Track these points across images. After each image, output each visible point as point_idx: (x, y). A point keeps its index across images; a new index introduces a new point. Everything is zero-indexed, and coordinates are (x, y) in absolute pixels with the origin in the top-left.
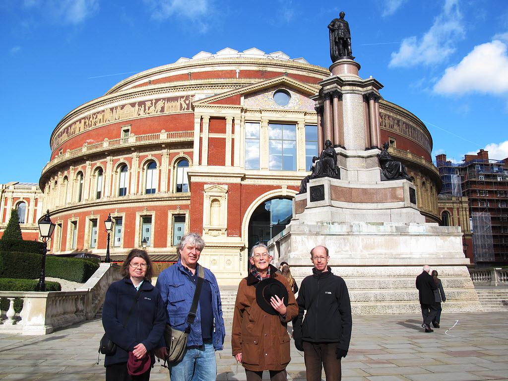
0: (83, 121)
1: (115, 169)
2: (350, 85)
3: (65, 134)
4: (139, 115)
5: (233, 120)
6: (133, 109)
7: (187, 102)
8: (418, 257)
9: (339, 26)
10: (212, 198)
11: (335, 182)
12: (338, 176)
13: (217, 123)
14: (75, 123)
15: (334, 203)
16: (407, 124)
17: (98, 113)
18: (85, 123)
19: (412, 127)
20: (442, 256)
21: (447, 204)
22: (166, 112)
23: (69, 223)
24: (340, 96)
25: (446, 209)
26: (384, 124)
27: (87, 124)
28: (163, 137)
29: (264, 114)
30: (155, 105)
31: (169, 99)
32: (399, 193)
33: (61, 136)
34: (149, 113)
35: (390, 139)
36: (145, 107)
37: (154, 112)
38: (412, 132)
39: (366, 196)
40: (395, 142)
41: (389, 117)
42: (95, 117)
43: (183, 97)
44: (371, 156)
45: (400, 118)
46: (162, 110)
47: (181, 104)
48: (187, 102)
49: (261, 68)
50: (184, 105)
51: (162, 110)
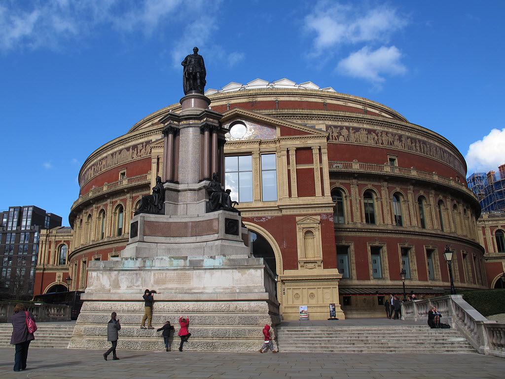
2: (186, 119)
4: (133, 158)
8: (210, 292)
9: (190, 61)
11: (152, 217)
12: (160, 211)
14: (88, 170)
15: (146, 238)
16: (412, 139)
17: (103, 159)
19: (420, 141)
20: (238, 291)
21: (501, 222)
23: (81, 263)
24: (176, 132)
25: (500, 228)
26: (380, 141)
34: (140, 156)
35: (389, 157)
36: (137, 150)
41: (387, 133)
44: (200, 189)
45: (403, 133)
49: (251, 100)
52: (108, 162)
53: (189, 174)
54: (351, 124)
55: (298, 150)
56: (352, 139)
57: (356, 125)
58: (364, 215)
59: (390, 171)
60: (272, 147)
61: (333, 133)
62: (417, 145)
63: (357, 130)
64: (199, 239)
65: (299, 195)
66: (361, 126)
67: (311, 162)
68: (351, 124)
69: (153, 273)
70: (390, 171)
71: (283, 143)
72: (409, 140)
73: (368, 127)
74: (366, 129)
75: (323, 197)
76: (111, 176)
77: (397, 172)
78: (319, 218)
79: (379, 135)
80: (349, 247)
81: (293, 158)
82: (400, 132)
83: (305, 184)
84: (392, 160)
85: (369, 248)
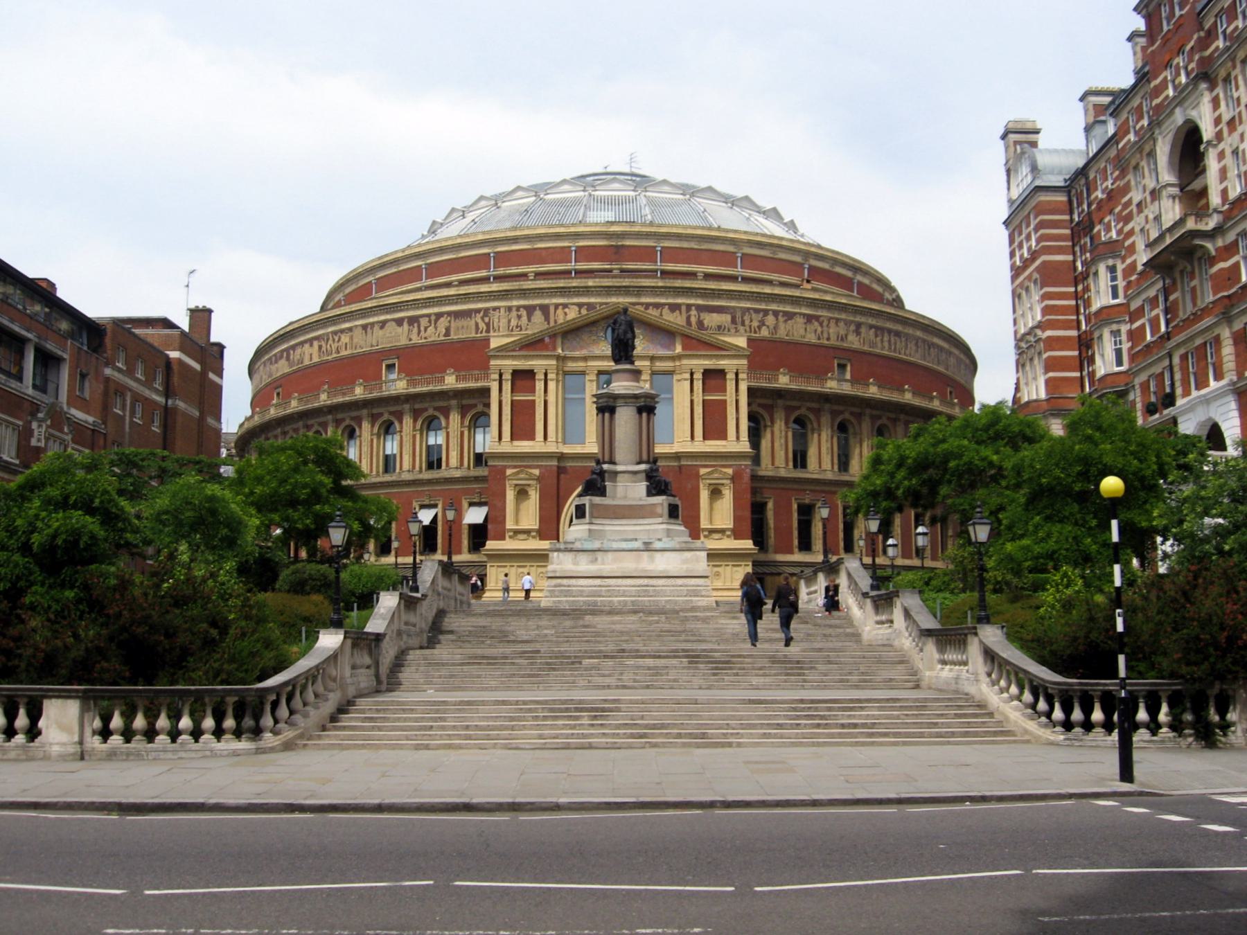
0: (316, 344)
1: (376, 430)
3: (283, 362)
5: (546, 374)
6: (399, 330)
7: (487, 320)
11: (597, 500)
12: (602, 492)
13: (523, 378)
14: (302, 343)
16: (877, 328)
17: (342, 331)
18: (320, 347)
19: (890, 331)
22: (453, 336)
27: (324, 349)
28: (451, 381)
29: (591, 363)
31: (458, 315)
32: (659, 510)
33: (276, 362)
37: (434, 334)
40: (849, 368)
41: (837, 320)
43: (478, 311)
47: (477, 324)
48: (487, 320)
50: (482, 326)
51: (447, 333)
52: (355, 340)
55: (707, 373)
56: (782, 334)
57: (788, 309)
60: (667, 365)
62: (886, 339)
63: (789, 316)
65: (706, 437)
67: (724, 390)
69: (610, 555)
71: (685, 362)
72: (872, 332)
74: (804, 315)
75: (736, 442)
76: (366, 365)
77: (847, 389)
78: (730, 471)
80: (766, 503)
81: (698, 385)
82: (858, 319)
83: (714, 425)
84: (842, 367)
85: (795, 506)
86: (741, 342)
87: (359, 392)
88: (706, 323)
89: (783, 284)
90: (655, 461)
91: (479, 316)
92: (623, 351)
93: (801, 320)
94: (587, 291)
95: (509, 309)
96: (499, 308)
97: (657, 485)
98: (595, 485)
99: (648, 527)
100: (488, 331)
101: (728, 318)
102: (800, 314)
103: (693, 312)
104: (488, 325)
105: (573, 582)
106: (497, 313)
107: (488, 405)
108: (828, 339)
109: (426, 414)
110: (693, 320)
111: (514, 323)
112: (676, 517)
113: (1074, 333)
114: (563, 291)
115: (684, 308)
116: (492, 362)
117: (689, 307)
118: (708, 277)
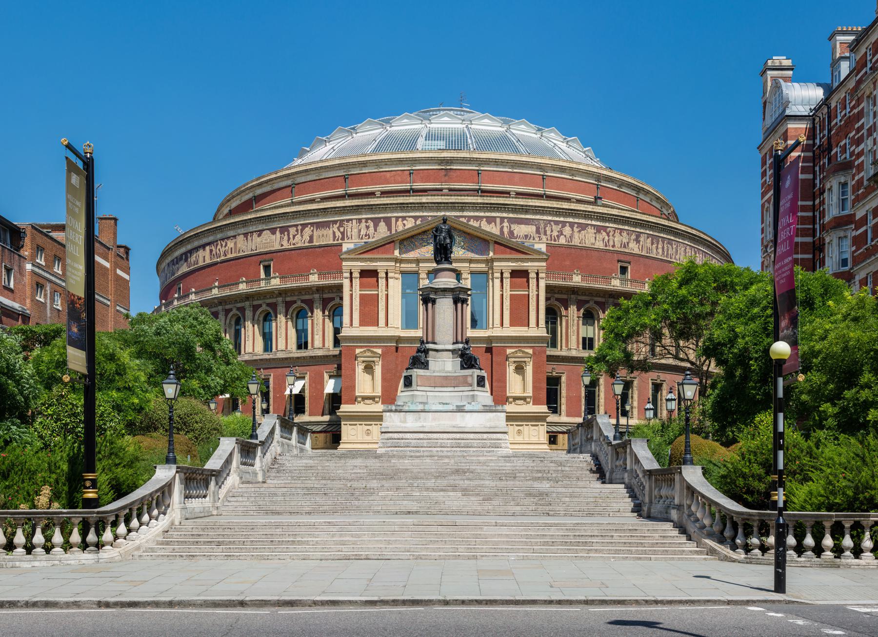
0: (208, 248)
5: (387, 273)
6: (273, 237)
7: (342, 229)
10: (364, 364)
12: (425, 365)
15: (419, 388)
18: (211, 251)
22: (315, 243)
24: (434, 302)
26: (611, 243)
27: (214, 252)
28: (314, 279)
30: (302, 232)
32: (469, 380)
33: (177, 263)
37: (300, 241)
38: (663, 248)
39: (446, 381)
42: (224, 244)
43: (335, 222)
46: (311, 241)
47: (334, 233)
48: (342, 229)
50: (338, 234)
51: (311, 241)
52: (239, 245)
53: (445, 337)
54: (576, 220)
55: (515, 274)
56: (576, 242)
58: (581, 340)
59: (618, 285)
61: (552, 231)
62: (660, 246)
64: (456, 389)
66: (589, 222)
68: (576, 220)
70: (618, 285)
73: (598, 223)
74: (594, 226)
79: (611, 234)
81: (507, 282)
84: (624, 270)
86: (543, 247)
87: (243, 287)
88: (515, 233)
89: (579, 201)
90: (467, 342)
91: (336, 226)
92: (443, 253)
93: (593, 231)
94: (421, 206)
95: (360, 221)
96: (351, 220)
97: (468, 361)
98: (419, 360)
99: (461, 394)
100: (343, 239)
101: (534, 228)
102: (592, 225)
103: (506, 224)
104: (343, 233)
105: (401, 435)
106: (350, 224)
107: (341, 298)
108: (613, 246)
109: (295, 306)
110: (506, 230)
111: (363, 232)
112: (483, 386)
113: (809, 239)
114: (403, 207)
115: (498, 220)
116: (344, 263)
117: (502, 219)
118: (519, 194)
